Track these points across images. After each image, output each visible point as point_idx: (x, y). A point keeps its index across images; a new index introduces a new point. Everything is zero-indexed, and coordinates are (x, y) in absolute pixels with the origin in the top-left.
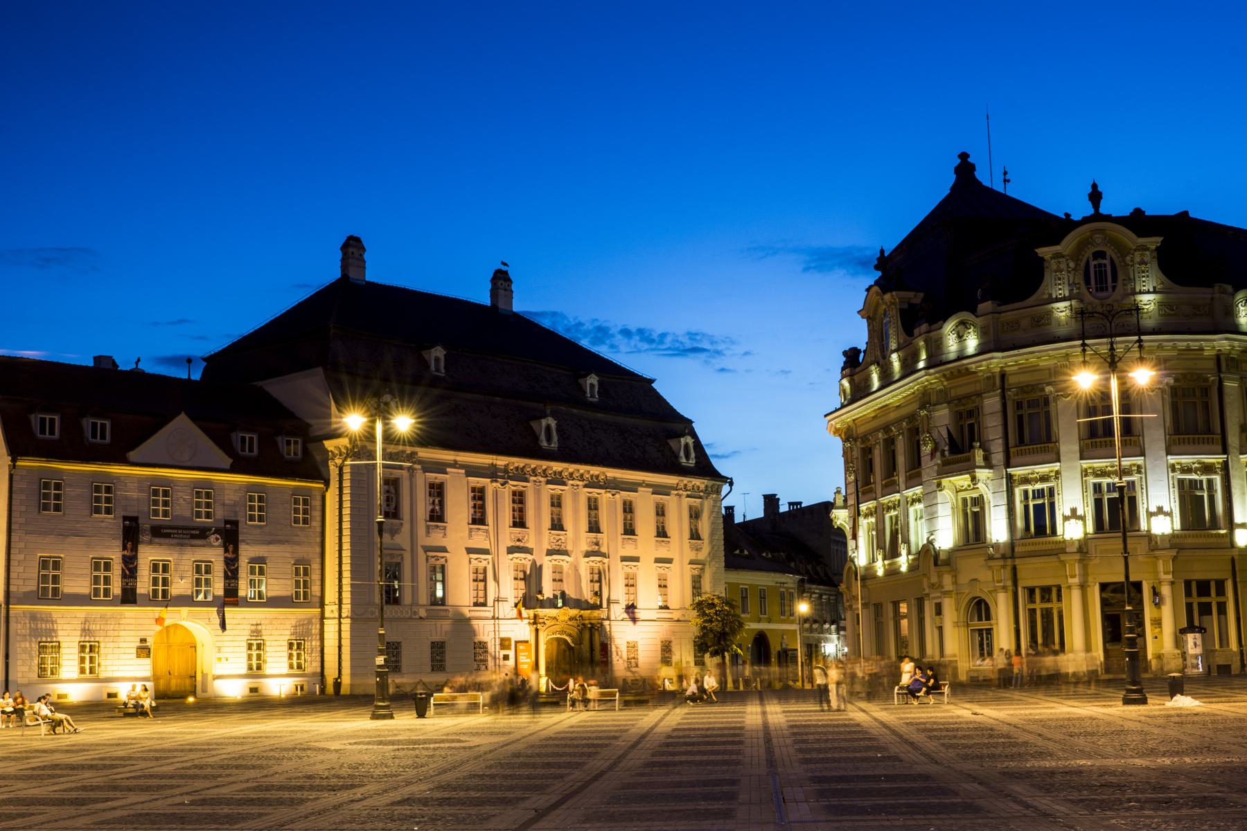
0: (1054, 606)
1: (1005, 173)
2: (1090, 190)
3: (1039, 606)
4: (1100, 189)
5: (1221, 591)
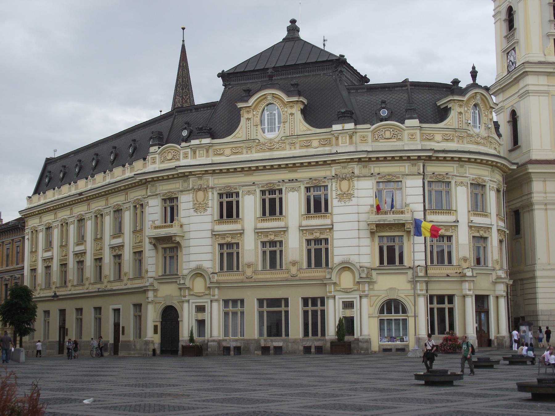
0: (446, 306)
2: (471, 70)
3: (435, 306)
4: (476, 69)
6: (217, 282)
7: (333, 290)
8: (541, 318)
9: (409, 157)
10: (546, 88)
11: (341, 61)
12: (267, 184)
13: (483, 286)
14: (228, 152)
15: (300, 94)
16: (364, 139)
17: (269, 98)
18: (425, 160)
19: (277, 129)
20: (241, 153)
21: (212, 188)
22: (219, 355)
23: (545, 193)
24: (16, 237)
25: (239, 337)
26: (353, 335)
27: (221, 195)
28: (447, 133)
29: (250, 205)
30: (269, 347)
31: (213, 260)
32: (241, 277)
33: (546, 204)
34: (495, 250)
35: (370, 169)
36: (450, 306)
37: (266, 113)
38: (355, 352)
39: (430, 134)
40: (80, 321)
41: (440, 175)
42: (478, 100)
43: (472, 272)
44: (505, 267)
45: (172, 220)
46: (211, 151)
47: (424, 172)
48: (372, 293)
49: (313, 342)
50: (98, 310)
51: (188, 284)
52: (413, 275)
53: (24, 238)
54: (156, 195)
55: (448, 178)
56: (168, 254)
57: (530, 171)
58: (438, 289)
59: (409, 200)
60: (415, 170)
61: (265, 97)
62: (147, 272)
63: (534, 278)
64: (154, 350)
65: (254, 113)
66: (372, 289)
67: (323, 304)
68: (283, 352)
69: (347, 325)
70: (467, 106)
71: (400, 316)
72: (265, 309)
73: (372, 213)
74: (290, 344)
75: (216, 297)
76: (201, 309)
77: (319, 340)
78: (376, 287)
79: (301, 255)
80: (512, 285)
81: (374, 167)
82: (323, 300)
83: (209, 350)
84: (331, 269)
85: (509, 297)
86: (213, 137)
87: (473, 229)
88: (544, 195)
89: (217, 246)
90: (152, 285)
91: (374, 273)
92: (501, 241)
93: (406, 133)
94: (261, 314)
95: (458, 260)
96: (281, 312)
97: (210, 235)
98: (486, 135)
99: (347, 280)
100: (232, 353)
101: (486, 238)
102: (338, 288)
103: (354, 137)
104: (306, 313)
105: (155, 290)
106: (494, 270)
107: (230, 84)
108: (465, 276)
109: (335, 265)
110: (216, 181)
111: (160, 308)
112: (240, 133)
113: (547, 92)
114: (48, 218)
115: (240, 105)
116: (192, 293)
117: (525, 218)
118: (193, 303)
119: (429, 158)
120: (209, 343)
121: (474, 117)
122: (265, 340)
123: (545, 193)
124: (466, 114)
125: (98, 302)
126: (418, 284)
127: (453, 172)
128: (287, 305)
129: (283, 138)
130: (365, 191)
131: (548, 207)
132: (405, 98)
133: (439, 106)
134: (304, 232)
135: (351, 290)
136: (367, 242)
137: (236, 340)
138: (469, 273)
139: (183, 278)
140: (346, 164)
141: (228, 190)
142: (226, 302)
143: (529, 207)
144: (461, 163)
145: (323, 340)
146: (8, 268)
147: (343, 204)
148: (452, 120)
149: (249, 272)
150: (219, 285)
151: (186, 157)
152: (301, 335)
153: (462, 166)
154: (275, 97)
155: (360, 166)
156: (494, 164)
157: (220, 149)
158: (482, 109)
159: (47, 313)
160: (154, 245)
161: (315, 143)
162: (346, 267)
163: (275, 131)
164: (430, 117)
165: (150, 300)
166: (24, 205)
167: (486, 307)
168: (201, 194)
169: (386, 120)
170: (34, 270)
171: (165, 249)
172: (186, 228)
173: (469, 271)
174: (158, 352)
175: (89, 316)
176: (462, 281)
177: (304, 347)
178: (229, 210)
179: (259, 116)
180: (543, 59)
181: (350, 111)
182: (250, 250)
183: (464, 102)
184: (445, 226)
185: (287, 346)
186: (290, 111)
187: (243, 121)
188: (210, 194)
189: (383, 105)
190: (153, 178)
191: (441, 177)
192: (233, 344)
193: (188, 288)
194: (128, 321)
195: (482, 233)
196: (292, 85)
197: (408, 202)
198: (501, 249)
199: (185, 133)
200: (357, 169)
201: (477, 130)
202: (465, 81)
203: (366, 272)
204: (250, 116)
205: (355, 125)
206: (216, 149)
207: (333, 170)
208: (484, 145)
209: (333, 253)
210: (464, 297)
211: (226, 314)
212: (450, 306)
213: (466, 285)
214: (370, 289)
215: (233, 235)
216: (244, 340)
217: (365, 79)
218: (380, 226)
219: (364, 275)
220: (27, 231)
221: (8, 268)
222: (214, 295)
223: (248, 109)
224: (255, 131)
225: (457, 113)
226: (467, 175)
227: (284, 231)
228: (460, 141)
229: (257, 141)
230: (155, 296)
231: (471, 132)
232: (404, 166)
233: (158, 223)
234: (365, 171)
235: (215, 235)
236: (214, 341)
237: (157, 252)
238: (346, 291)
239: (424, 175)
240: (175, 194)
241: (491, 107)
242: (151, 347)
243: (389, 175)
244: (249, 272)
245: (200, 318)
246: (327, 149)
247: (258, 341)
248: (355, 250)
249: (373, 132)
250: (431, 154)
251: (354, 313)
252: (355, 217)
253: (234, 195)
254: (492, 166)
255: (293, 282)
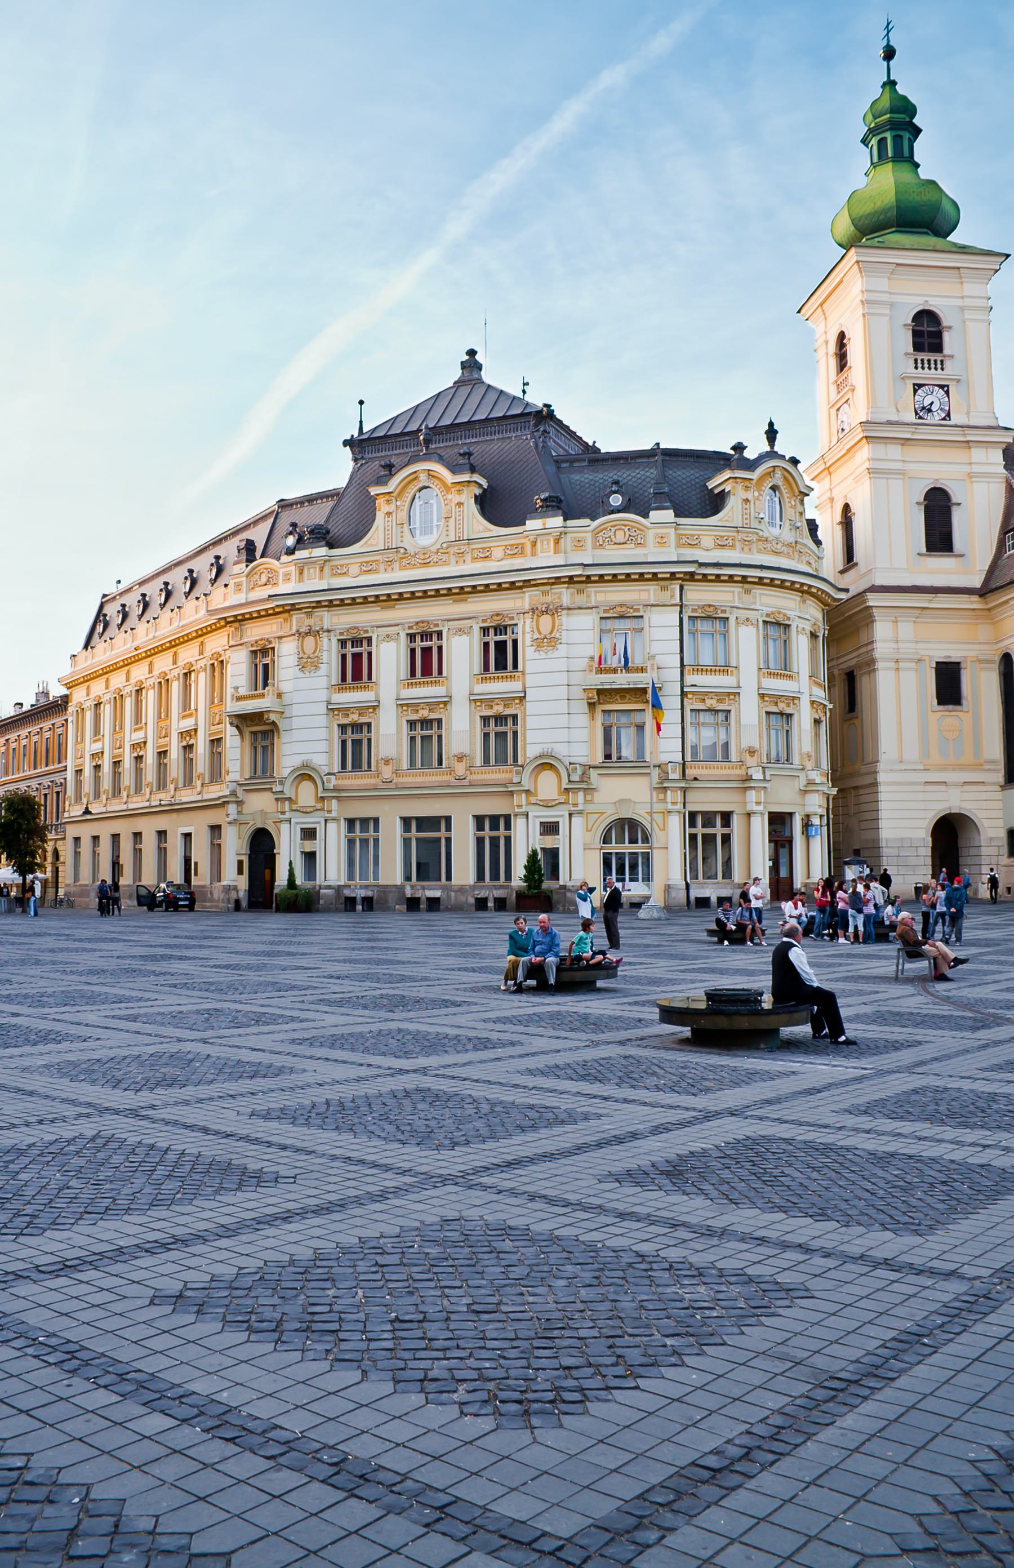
1: (525, 384)
2: (767, 428)
3: (700, 830)
4: (775, 427)
6: (335, 789)
7: (524, 803)
8: (885, 851)
9: (655, 574)
10: (898, 466)
11: (545, 416)
12: (417, 623)
13: (784, 797)
14: (354, 569)
15: (473, 470)
16: (579, 544)
17: (423, 477)
18: (683, 580)
19: (435, 530)
20: (377, 571)
21: (329, 631)
22: (337, 910)
23: (897, 642)
24: (58, 720)
25: (371, 881)
26: (558, 879)
27: (343, 643)
29: (390, 659)
30: (419, 898)
31: (329, 752)
32: (373, 781)
33: (897, 661)
34: (808, 739)
35: (589, 596)
36: (726, 830)
37: (417, 502)
38: (561, 908)
39: (694, 535)
40: (138, 853)
41: (710, 606)
42: (778, 479)
43: (764, 773)
44: (825, 764)
45: (265, 684)
46: (327, 569)
47: (681, 599)
48: (590, 808)
49: (491, 892)
50: (162, 834)
51: (289, 792)
52: (659, 778)
53: (66, 720)
54: (241, 644)
55: (724, 611)
56: (261, 743)
57: (871, 604)
58: (703, 802)
59: (656, 648)
60: (665, 597)
61: (414, 477)
62: (228, 772)
63: (875, 784)
64: (237, 902)
65: (398, 503)
66: (591, 802)
67: (508, 827)
68: (442, 907)
69: (545, 865)
70: (759, 490)
71: (639, 848)
72: (414, 833)
73: (591, 671)
74: (453, 894)
75: (334, 814)
76: (309, 834)
77: (501, 887)
78: (598, 797)
79: (472, 744)
80: (835, 798)
81: (596, 592)
82: (507, 819)
83: (321, 902)
84: (522, 766)
85: (831, 816)
86: (331, 546)
87: (766, 699)
88: (895, 646)
89: (336, 731)
90: (233, 793)
91: (593, 773)
92: (817, 722)
93: (651, 535)
94: (407, 842)
95: (740, 752)
96: (439, 840)
97: (325, 711)
98: (793, 540)
99: (548, 786)
100: (359, 907)
101: (789, 716)
102: (533, 800)
103: (562, 541)
104: (480, 841)
105: (240, 803)
106: (803, 769)
107: (362, 458)
108: (749, 779)
109: (528, 761)
110: (335, 620)
111: (247, 832)
112: (376, 538)
113: (902, 473)
114: (98, 688)
115: (374, 491)
116: (294, 807)
117: (863, 684)
118: (297, 823)
119: (691, 577)
120: (322, 891)
121: (772, 508)
122: (412, 887)
123: (897, 642)
125: (161, 823)
126: (669, 792)
127: (733, 601)
128: (448, 829)
129: (445, 545)
130: (581, 633)
131: (901, 665)
132: (653, 476)
133: (712, 489)
134: (478, 704)
135: (554, 803)
136: (583, 719)
137: (366, 887)
138: (758, 775)
139: (282, 783)
140: (548, 588)
141: (354, 634)
142: (351, 822)
143: (869, 664)
144: (746, 586)
145: (507, 887)
146: (47, 768)
147: (543, 655)
148: (731, 513)
149: (387, 772)
150: (339, 794)
151: (287, 578)
152: (471, 879)
153: (748, 592)
154: (433, 476)
155: (572, 590)
156: (806, 588)
157: (342, 566)
158: (786, 496)
159: (77, 840)
160: (237, 727)
161: (498, 553)
162: (546, 764)
163: (432, 533)
164: (695, 509)
165: (230, 819)
166: (65, 669)
167: (787, 834)
168: (310, 641)
169: (619, 511)
170: (79, 772)
171: (254, 734)
172: (286, 699)
173: (758, 772)
174: (244, 904)
175: (149, 845)
176: (746, 789)
177: (477, 899)
178: (356, 668)
179: (406, 508)
180: (894, 418)
181: (557, 497)
182: (389, 736)
183: (753, 482)
184: (717, 694)
185: (449, 897)
186: (457, 498)
187: (380, 516)
188: (325, 640)
189: (615, 488)
190: (235, 616)
191: (712, 609)
192: (362, 893)
193: (289, 799)
194: (201, 854)
195: (782, 706)
196: (461, 455)
197: (652, 652)
198: (817, 735)
199: (291, 541)
200: (565, 595)
201: (775, 531)
202: (756, 447)
203: (579, 772)
204: (391, 508)
205: (565, 520)
206: (336, 566)
207: (526, 599)
208: (788, 556)
209: (525, 740)
210: (749, 815)
211: (351, 842)
212: (726, 830)
213: (752, 795)
214: (586, 801)
215: (362, 710)
216: (378, 886)
217: (595, 450)
218: (604, 694)
219: (575, 777)
220: (70, 709)
221: (47, 768)
222: (330, 812)
223: (387, 497)
224: (400, 534)
225: (740, 501)
227: (445, 703)
228: (746, 549)
229: (402, 551)
230: (239, 813)
231: (766, 534)
232: (648, 590)
233: (243, 691)
234: (580, 600)
235: (332, 710)
236: (329, 887)
237: (242, 740)
238: (547, 805)
239: (681, 606)
240: (270, 642)
241: (801, 492)
242: (233, 895)
243: (621, 606)
244: (387, 772)
245: (308, 850)
246: (518, 563)
247: (401, 888)
248: (563, 735)
249: (596, 533)
250: (692, 570)
251: (559, 842)
252: (563, 678)
253: (365, 643)
254: (803, 592)
255: (462, 790)
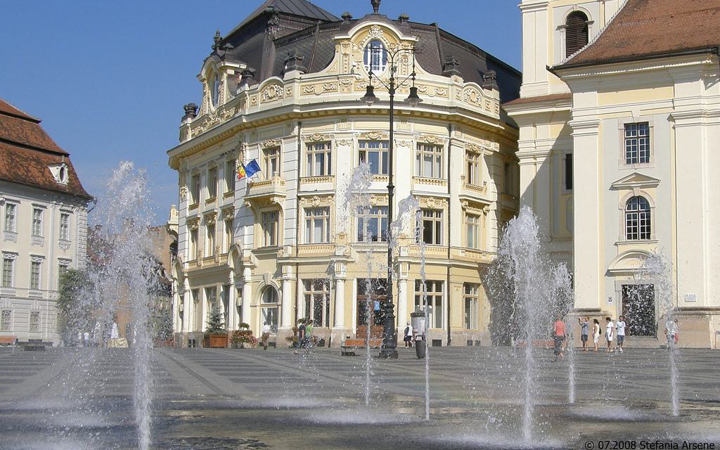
5: (439, 289)
28: (332, 81)
124: (355, 54)
225: (342, 55)
226: (353, 131)
232: (282, 128)
